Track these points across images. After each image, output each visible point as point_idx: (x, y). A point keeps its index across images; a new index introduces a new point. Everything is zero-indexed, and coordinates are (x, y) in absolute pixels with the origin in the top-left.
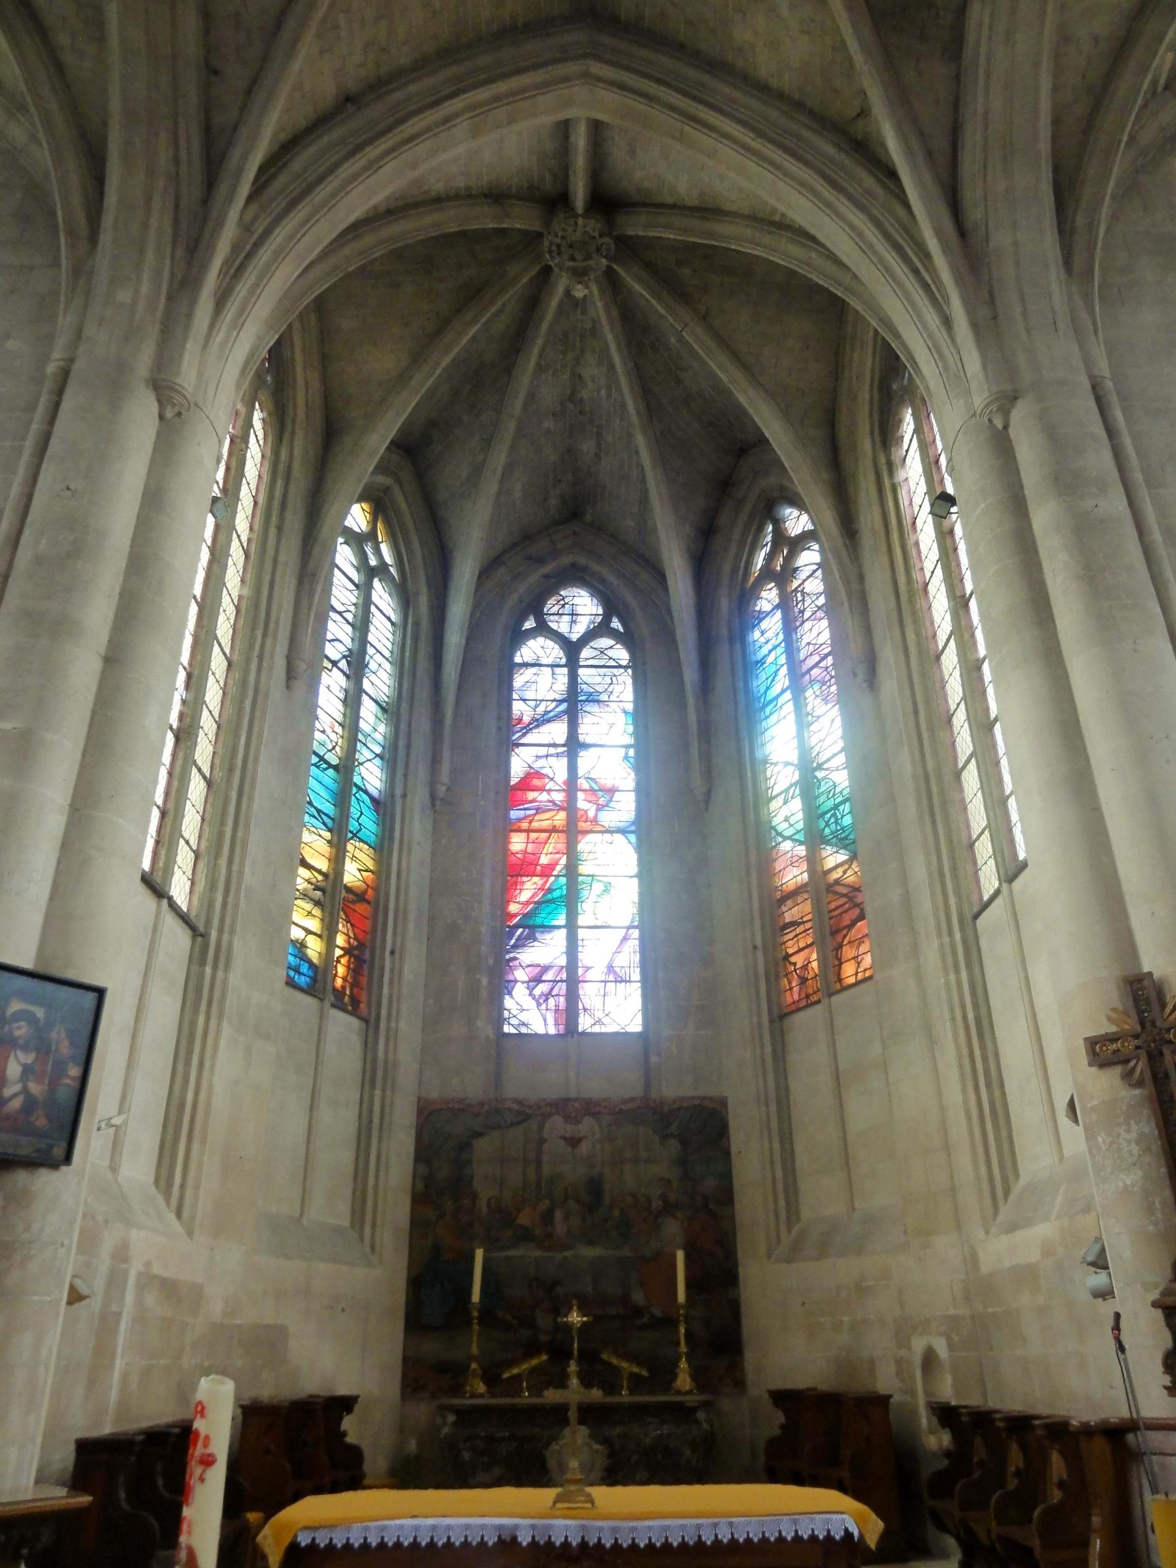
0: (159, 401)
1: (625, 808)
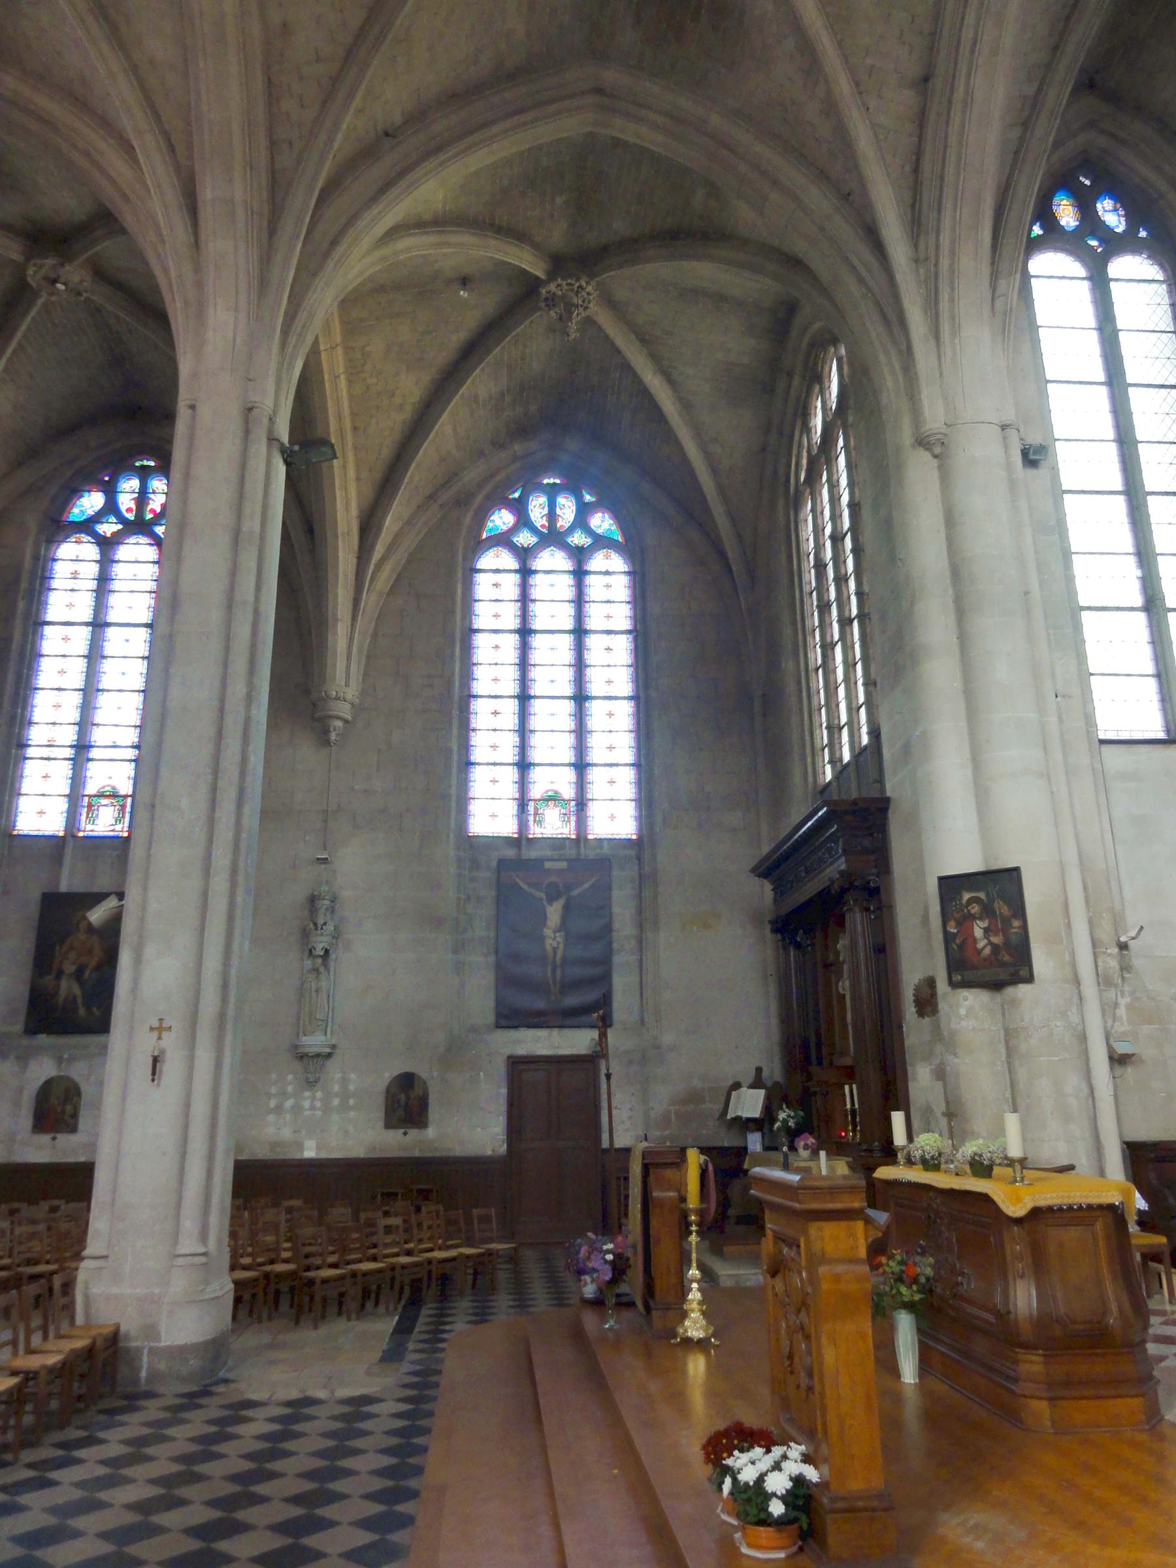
0: (927, 449)
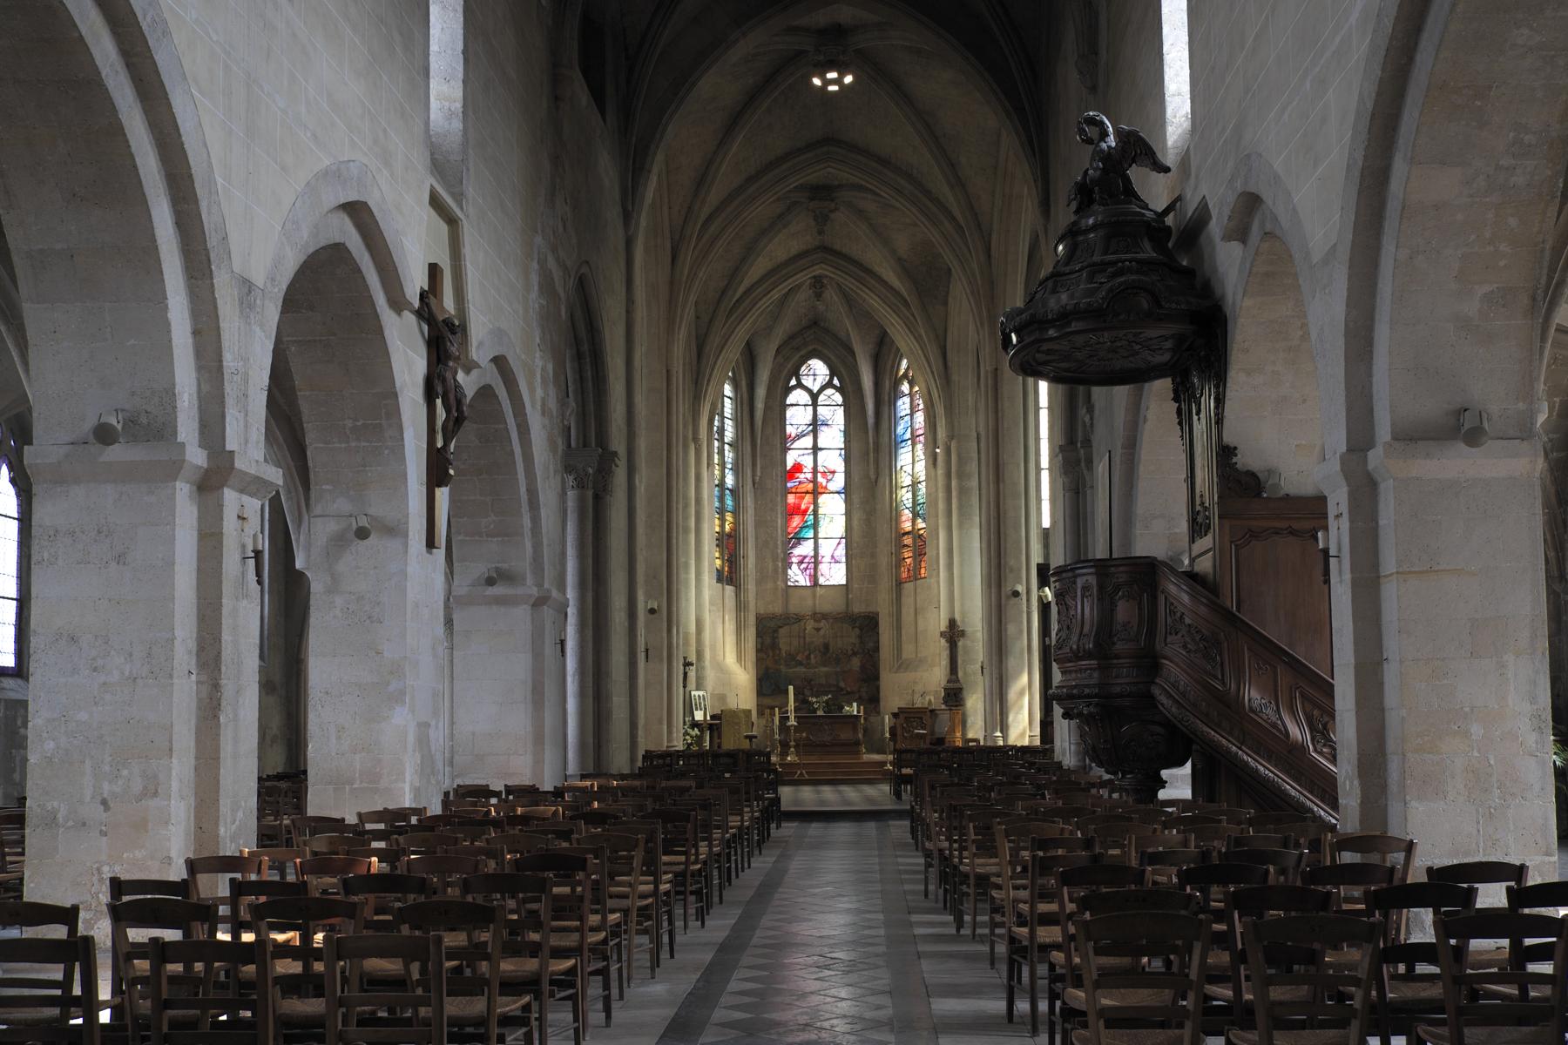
1: (839, 482)
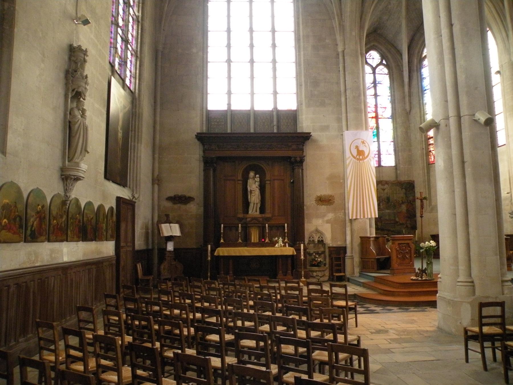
1: (389, 112)
